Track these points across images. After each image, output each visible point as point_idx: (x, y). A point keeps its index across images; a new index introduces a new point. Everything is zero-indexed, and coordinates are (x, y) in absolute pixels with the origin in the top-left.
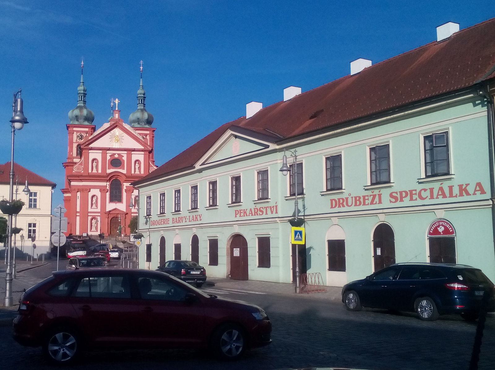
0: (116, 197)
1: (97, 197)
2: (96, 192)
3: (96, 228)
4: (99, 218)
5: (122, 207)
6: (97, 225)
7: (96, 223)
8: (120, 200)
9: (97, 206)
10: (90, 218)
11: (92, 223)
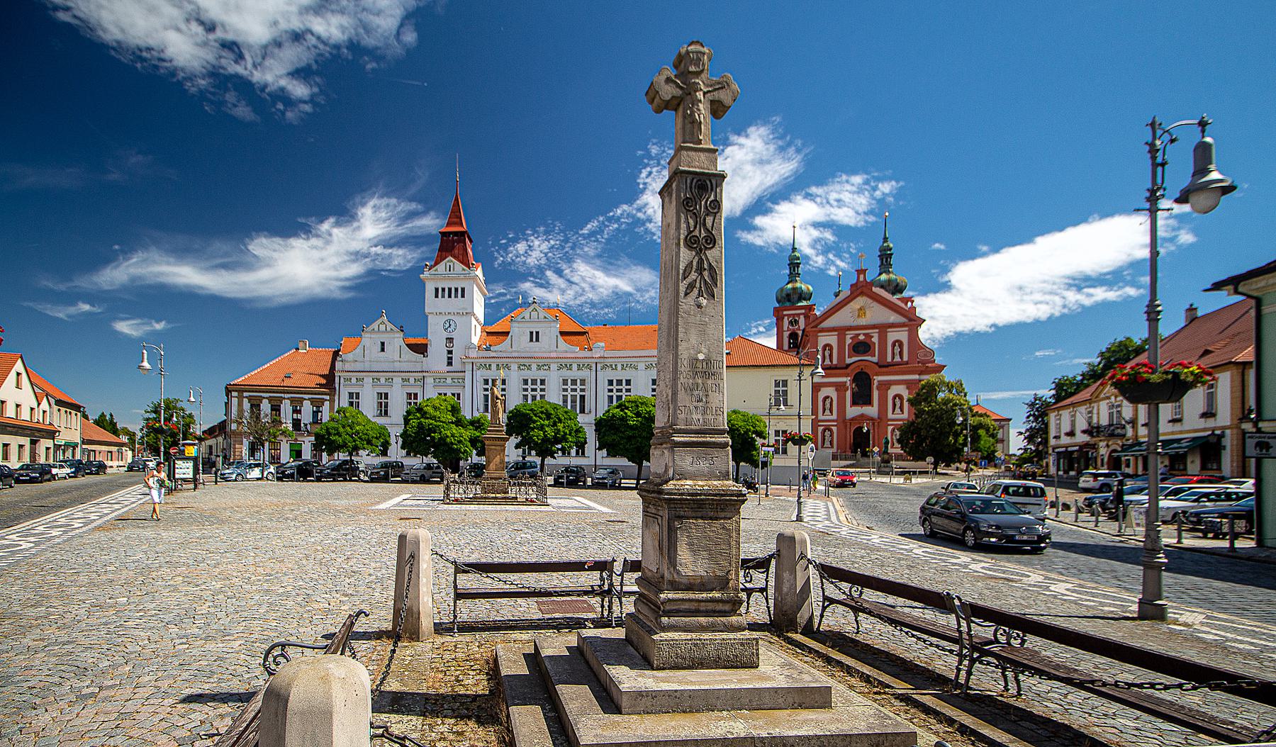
0: (862, 397)
3: (831, 443)
4: (834, 429)
5: (872, 411)
8: (868, 401)
9: (831, 412)
11: (824, 436)
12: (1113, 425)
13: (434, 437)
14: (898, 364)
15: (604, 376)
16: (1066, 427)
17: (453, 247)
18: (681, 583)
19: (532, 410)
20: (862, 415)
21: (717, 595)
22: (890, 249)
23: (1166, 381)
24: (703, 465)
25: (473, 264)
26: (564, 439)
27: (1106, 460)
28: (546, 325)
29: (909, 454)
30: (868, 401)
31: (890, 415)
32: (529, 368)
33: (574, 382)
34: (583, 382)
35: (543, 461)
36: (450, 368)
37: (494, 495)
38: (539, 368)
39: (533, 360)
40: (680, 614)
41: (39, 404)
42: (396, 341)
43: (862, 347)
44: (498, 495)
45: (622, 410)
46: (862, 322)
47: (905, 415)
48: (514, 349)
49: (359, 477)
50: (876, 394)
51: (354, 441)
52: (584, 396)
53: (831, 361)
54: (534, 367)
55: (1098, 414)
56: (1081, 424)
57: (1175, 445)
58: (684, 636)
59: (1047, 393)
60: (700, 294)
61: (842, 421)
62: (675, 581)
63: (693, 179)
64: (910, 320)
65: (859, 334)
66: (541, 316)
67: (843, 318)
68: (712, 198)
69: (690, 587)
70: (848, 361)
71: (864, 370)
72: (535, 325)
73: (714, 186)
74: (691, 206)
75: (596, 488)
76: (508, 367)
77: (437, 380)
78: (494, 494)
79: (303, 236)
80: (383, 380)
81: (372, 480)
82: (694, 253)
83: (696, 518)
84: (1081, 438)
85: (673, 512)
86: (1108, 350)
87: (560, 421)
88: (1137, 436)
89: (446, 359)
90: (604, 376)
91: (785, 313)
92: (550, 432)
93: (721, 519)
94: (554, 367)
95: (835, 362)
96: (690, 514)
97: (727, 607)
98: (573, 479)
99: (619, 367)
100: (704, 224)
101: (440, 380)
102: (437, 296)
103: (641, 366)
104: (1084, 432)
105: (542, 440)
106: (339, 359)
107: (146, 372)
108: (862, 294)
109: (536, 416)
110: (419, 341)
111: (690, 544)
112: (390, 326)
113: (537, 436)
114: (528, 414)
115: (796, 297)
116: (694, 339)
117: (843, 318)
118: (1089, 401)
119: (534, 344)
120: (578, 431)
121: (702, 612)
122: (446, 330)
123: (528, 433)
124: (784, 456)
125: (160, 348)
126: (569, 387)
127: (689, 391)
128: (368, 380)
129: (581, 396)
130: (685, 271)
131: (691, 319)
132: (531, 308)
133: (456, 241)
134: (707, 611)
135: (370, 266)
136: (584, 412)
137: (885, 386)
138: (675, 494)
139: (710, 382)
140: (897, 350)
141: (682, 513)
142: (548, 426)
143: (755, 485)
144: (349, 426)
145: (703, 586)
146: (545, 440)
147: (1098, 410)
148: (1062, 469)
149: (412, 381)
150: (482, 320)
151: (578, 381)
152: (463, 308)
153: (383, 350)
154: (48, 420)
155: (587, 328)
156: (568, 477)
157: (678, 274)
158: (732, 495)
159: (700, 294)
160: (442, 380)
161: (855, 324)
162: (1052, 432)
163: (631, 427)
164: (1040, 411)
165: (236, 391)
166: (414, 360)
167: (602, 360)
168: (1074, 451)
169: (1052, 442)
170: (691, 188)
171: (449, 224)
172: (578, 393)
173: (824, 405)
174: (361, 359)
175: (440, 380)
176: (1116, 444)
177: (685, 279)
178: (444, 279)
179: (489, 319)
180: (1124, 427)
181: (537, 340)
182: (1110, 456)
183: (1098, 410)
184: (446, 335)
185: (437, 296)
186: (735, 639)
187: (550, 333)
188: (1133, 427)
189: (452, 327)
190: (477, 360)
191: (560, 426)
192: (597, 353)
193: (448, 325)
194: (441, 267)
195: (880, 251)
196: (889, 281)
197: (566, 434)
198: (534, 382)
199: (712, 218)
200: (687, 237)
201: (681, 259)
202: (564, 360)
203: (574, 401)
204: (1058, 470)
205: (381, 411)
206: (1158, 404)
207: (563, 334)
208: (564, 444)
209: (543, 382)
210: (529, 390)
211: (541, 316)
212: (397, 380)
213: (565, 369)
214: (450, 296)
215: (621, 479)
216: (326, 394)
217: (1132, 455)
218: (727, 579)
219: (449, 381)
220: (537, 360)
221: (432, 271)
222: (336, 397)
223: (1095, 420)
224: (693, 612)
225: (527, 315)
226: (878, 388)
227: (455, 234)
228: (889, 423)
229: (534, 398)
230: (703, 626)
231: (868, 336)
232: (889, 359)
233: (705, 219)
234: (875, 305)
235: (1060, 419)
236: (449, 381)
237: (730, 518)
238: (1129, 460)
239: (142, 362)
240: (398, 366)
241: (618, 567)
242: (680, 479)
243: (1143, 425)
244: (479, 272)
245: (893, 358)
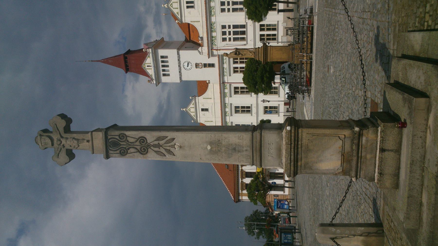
42: (202, 101)
119: (196, 4)
153: (207, 110)
165: (238, 197)
181: (192, 2)
185: (168, 75)
214: (168, 66)
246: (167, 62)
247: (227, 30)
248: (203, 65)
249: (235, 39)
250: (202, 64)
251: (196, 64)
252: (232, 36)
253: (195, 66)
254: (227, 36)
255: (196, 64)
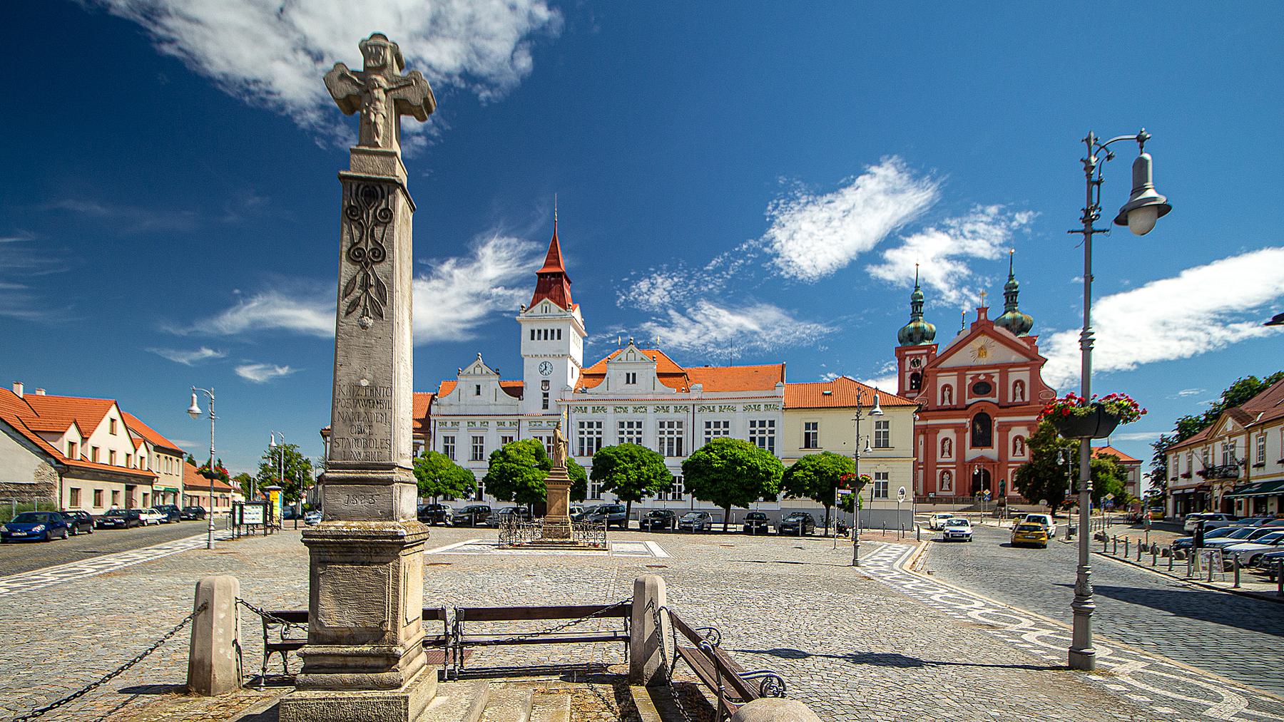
0: (982, 439)
1: (950, 441)
2: (950, 434)
3: (950, 486)
4: (953, 471)
5: (992, 453)
6: (951, 482)
7: (950, 478)
8: (989, 444)
9: (950, 454)
10: (939, 472)
11: (943, 479)
12: (1226, 466)
13: (515, 481)
14: (1019, 405)
15: (702, 418)
16: (1183, 469)
17: (550, 289)
18: (327, 636)
19: (616, 453)
20: (982, 458)
21: (365, 649)
22: (1016, 287)
23: (1090, 414)
24: (361, 504)
25: (569, 305)
26: (648, 482)
27: (1219, 502)
28: (644, 366)
29: (1026, 497)
30: (989, 444)
31: (1011, 458)
32: (626, 410)
33: (671, 425)
34: (680, 424)
35: (629, 505)
36: (545, 411)
37: (550, 540)
38: (636, 410)
39: (629, 402)
40: (322, 670)
41: (136, 450)
42: (492, 384)
43: (982, 388)
44: (554, 540)
45: (707, 453)
46: (983, 361)
47: (1026, 458)
48: (610, 391)
49: (445, 522)
50: (996, 435)
51: (437, 486)
52: (681, 438)
53: (950, 402)
54: (630, 409)
55: (1213, 454)
56: (1198, 466)
57: (1248, 490)
58: (321, 694)
59: (1172, 434)
60: (365, 313)
61: (963, 465)
62: (319, 634)
63: (359, 186)
64: (1033, 359)
65: (980, 375)
66: (638, 358)
67: (963, 357)
68: (383, 206)
69: (336, 641)
70: (968, 402)
71: (986, 412)
72: (633, 366)
73: (386, 194)
74: (355, 216)
75: (683, 533)
76: (604, 410)
77: (533, 424)
78: (556, 539)
79: (423, 277)
80: (478, 424)
81: (456, 525)
82: (358, 267)
83: (343, 563)
84: (1197, 480)
85: (317, 557)
86: (1232, 389)
87: (644, 464)
88: (1249, 477)
89: (542, 401)
90: (702, 418)
91: (906, 353)
92: (633, 476)
93: (375, 563)
94: (651, 409)
95: (954, 403)
96: (338, 558)
97: (381, 662)
98: (660, 523)
99: (717, 408)
100: (372, 236)
101: (535, 424)
102: (533, 338)
103: (740, 408)
104: (1199, 473)
105: (625, 483)
106: (434, 402)
107: (196, 416)
108: (983, 333)
109: (619, 458)
110: (517, 384)
111: (335, 592)
112: (485, 369)
113: (620, 480)
114: (612, 457)
115: (918, 337)
116: (356, 364)
117: (963, 357)
118: (1204, 442)
119: (631, 386)
120: (663, 474)
121: (351, 667)
122: (541, 372)
123: (611, 477)
124: (885, 499)
125: (211, 392)
126: (666, 429)
127: (348, 422)
128: (463, 424)
129: (678, 438)
130: (347, 287)
131: (354, 341)
132: (627, 350)
133: (553, 282)
134: (356, 667)
135: (492, 307)
136: (681, 455)
137: (1005, 428)
138: (315, 537)
139: (374, 411)
140: (1018, 390)
141: (328, 558)
142: (632, 470)
143: (846, 529)
144: (432, 470)
145: (352, 639)
146: (628, 484)
147: (1213, 450)
148: (1179, 511)
149: (507, 424)
150: (581, 364)
151: (676, 423)
152: (559, 351)
153: (478, 393)
154: (133, 463)
155: (685, 370)
156: (653, 521)
157: (339, 292)
158: (386, 537)
159: (365, 313)
160: (538, 424)
161: (975, 363)
162: (1170, 475)
163: (717, 470)
164: (1164, 450)
166: (509, 403)
167: (699, 402)
168: (1190, 493)
169: (1170, 484)
170: (357, 194)
171: (546, 265)
172: (675, 436)
173: (943, 447)
174: (456, 402)
175: (535, 424)
176: (1229, 486)
177: (346, 296)
178: (540, 320)
179: (587, 362)
180: (1237, 468)
182: (1223, 498)
183: (1213, 450)
184: (542, 377)
185: (533, 338)
186: (378, 698)
187: (647, 374)
188: (1245, 469)
189: (548, 369)
190: (572, 403)
191: (644, 469)
192: (694, 395)
193: (544, 368)
194: (537, 308)
195: (1006, 289)
196: (1014, 320)
197: (649, 477)
198: (631, 425)
199: (382, 229)
200: (349, 250)
201: (343, 274)
202: (660, 402)
203: (671, 444)
204: (1175, 512)
205: (476, 455)
206: (1090, 439)
207: (660, 375)
208: (647, 488)
209: (639, 425)
210: (626, 433)
211: (638, 358)
212: (493, 424)
213: (662, 412)
214: (546, 338)
215: (711, 523)
216: (421, 439)
217: (1242, 497)
218: (382, 630)
219: (545, 424)
220: (634, 403)
221: (528, 313)
222: (432, 442)
223: (1210, 462)
224: (339, 668)
225: (623, 356)
226: (998, 430)
227: (553, 274)
228: (1010, 465)
229: (630, 440)
230: (346, 683)
231: (989, 376)
232: (1010, 400)
233: (373, 230)
234: (997, 344)
235: (1177, 461)
236: (545, 424)
237: (385, 563)
238: (1240, 502)
239: (192, 405)
240: (493, 410)
241: (451, 614)
242: (332, 520)
243: (1254, 466)
244: (577, 314)
245: (1014, 398)
246: (552, 338)
247: (595, 429)
248: (546, 392)
249: (582, 440)
250: (549, 389)
251: (549, 381)
252: (586, 436)
253: (545, 379)
254: (586, 429)
255: (549, 381)
